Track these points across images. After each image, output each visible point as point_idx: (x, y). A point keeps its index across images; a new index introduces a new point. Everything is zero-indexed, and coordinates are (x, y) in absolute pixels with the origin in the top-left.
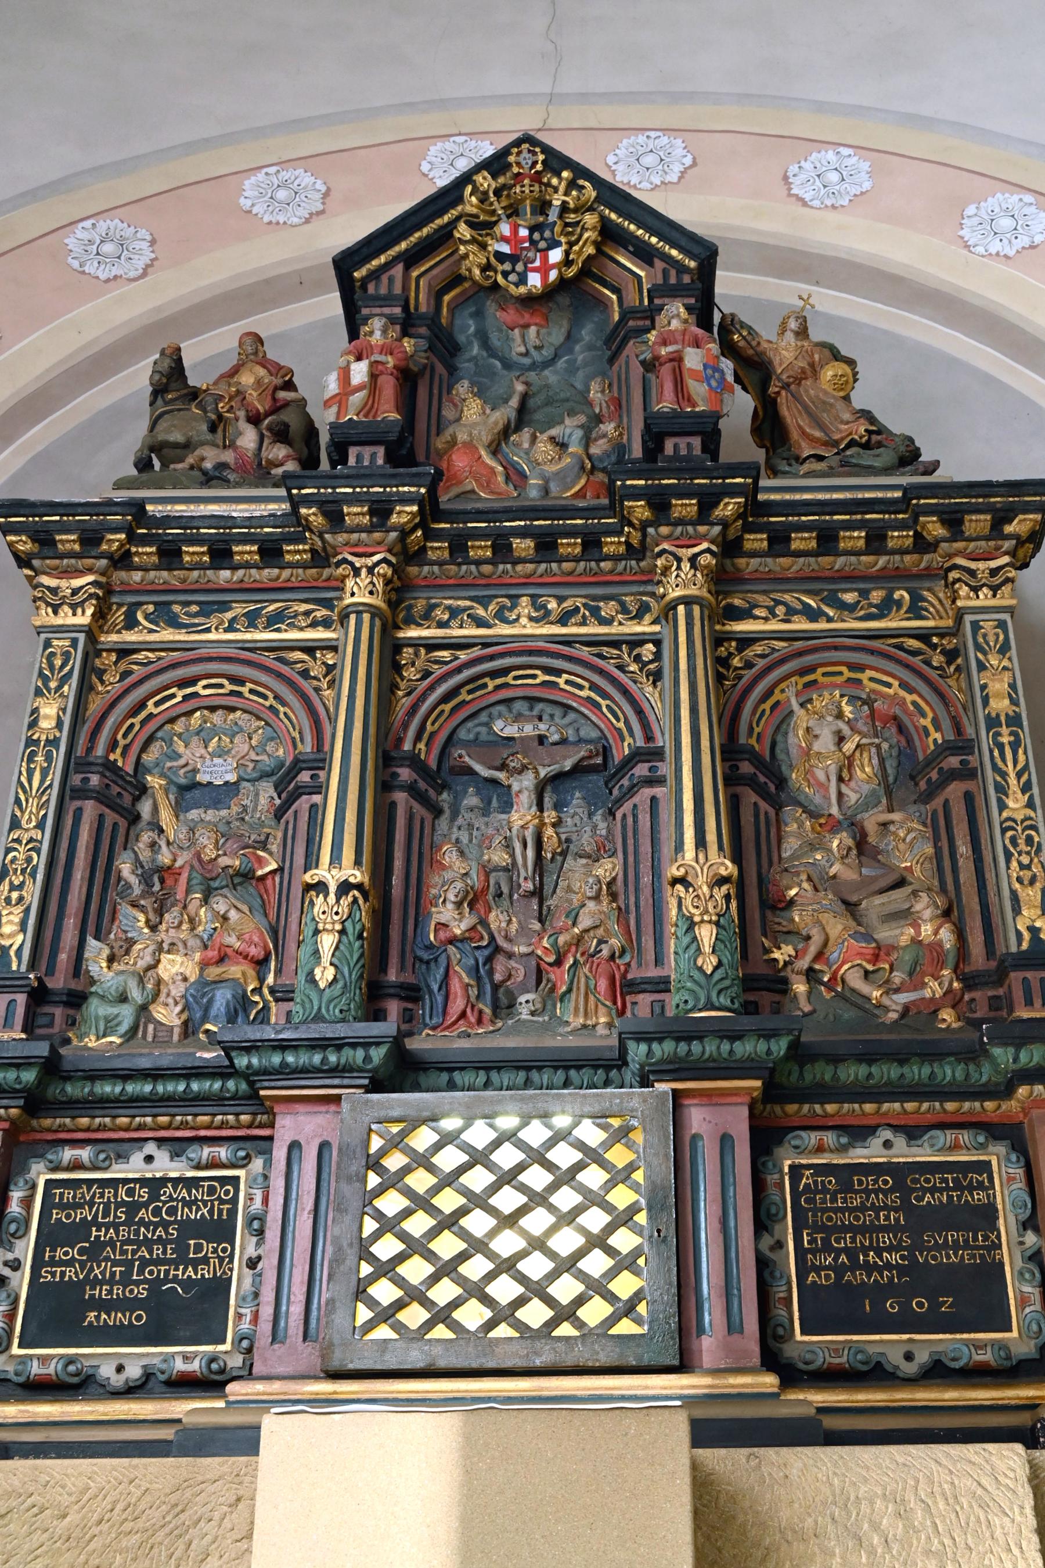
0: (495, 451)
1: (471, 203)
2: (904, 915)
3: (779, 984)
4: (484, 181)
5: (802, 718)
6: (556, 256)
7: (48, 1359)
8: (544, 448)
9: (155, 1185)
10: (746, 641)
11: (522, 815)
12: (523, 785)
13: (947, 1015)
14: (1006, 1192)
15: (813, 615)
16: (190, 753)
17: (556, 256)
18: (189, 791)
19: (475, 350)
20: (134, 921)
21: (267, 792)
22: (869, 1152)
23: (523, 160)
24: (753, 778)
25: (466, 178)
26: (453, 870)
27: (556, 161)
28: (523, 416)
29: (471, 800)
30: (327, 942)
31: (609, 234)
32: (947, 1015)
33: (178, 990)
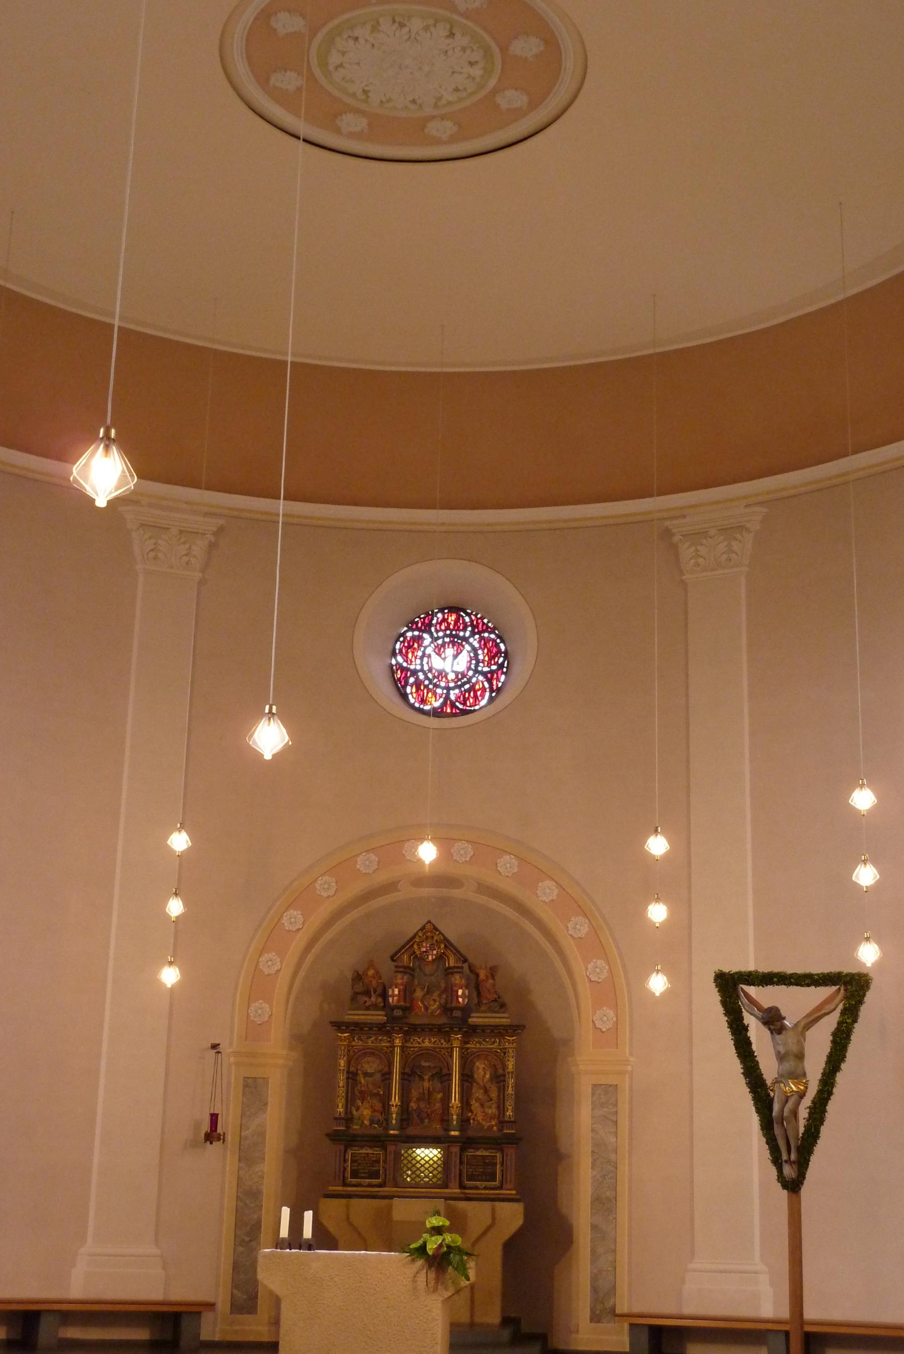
0: (422, 1001)
1: (417, 940)
2: (490, 1107)
3: (468, 1120)
4: (420, 934)
5: (477, 1064)
6: (435, 952)
7: (354, 1181)
8: (432, 1003)
9: (368, 1154)
10: (467, 1049)
11: (426, 1084)
12: (426, 1077)
13: (495, 1128)
14: (499, 1160)
15: (480, 1043)
16: (366, 1066)
17: (435, 952)
18: (366, 1074)
19: (418, 970)
20: (359, 1103)
21: (379, 1075)
22: (479, 1153)
23: (428, 927)
24: (467, 1078)
25: (417, 934)
26: (415, 1094)
27: (436, 929)
28: (428, 992)
29: (417, 1078)
30: (394, 1116)
31: (446, 946)
32: (495, 1128)
33: (368, 1117)
